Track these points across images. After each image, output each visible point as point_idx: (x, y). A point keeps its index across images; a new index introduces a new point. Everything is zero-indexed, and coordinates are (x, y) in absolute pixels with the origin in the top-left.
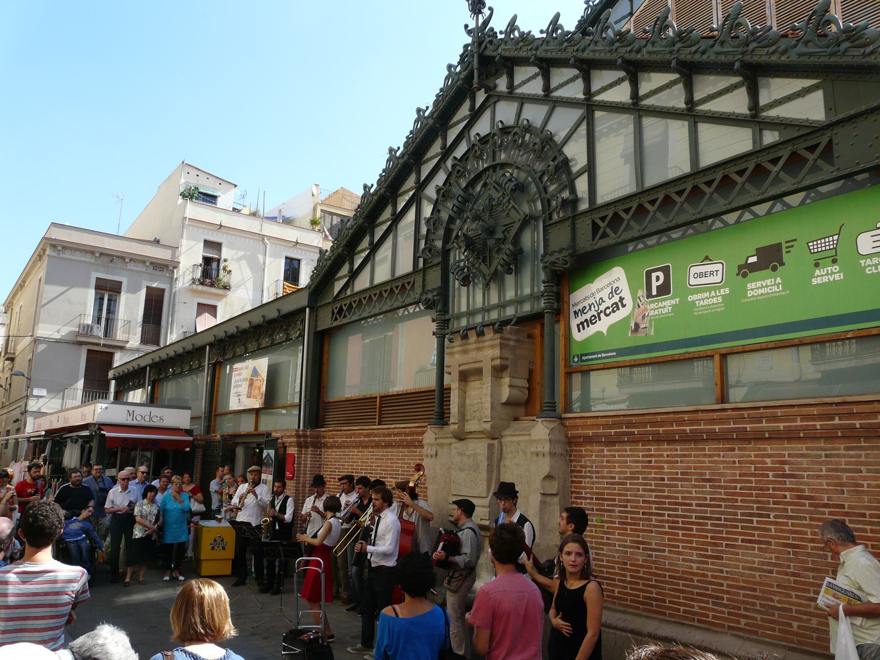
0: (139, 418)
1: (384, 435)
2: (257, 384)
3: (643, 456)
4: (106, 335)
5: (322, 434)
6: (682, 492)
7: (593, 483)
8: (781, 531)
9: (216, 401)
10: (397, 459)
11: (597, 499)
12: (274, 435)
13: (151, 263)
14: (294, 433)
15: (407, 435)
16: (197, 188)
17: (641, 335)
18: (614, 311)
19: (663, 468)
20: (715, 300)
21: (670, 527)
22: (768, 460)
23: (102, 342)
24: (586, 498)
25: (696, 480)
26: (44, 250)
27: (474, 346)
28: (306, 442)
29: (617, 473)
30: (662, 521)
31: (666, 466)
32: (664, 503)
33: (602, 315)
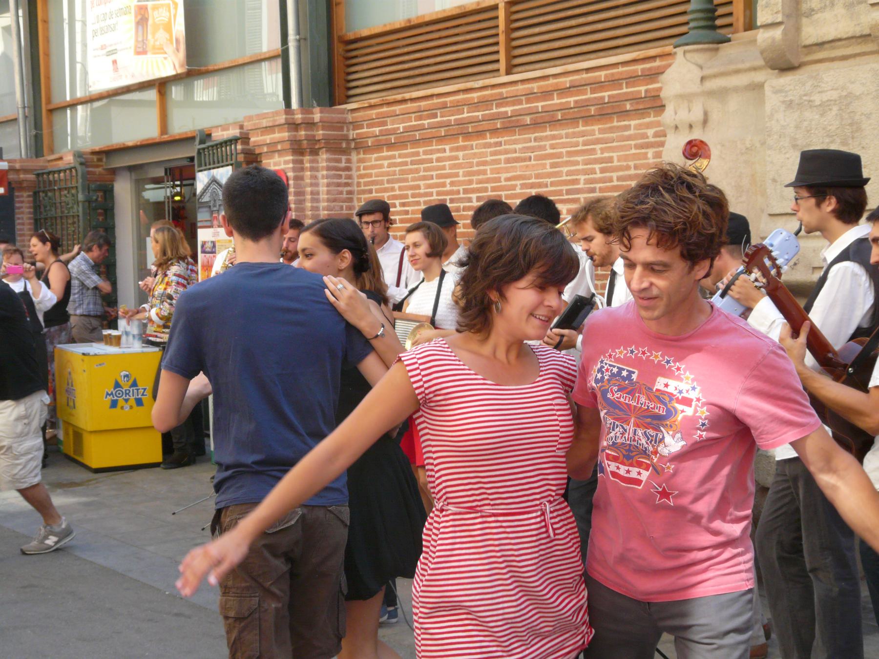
1: (531, 96)
5: (350, 117)
9: (48, 78)
10: (569, 154)
12: (219, 135)
14: (282, 119)
15: (598, 85)
28: (312, 140)
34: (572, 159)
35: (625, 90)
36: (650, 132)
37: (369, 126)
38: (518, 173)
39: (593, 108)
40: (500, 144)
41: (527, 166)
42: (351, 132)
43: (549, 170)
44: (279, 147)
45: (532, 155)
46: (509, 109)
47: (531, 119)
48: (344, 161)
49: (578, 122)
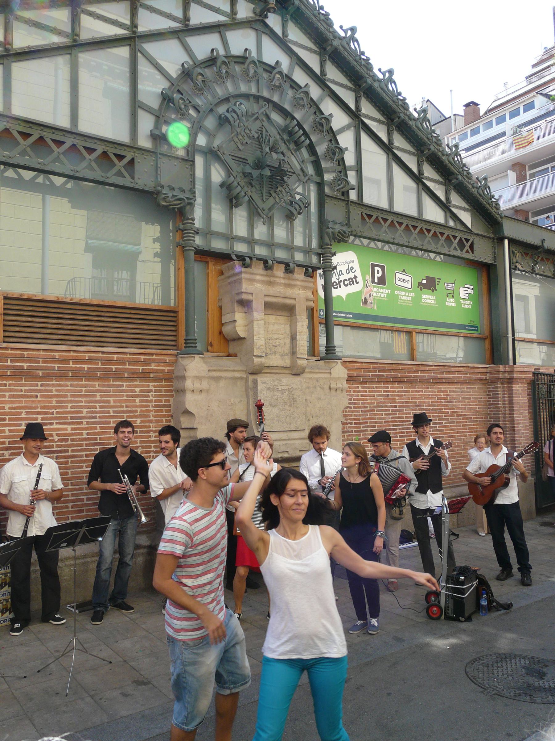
3: (384, 392)
6: (406, 414)
7: (352, 412)
8: (447, 430)
10: (72, 396)
11: (355, 423)
17: (368, 307)
18: (351, 285)
19: (395, 399)
20: (408, 298)
21: (400, 436)
22: (442, 394)
24: (347, 424)
25: (413, 406)
27: (283, 281)
29: (368, 403)
30: (396, 433)
31: (397, 398)
32: (396, 421)
33: (342, 284)
34: (76, 399)
35: (127, 367)
36: (137, 390)
38: (23, 405)
39: (99, 373)
40: (5, 385)
41: (33, 401)
43: (54, 404)
45: (39, 395)
46: (25, 365)
47: (43, 373)
49: (82, 379)
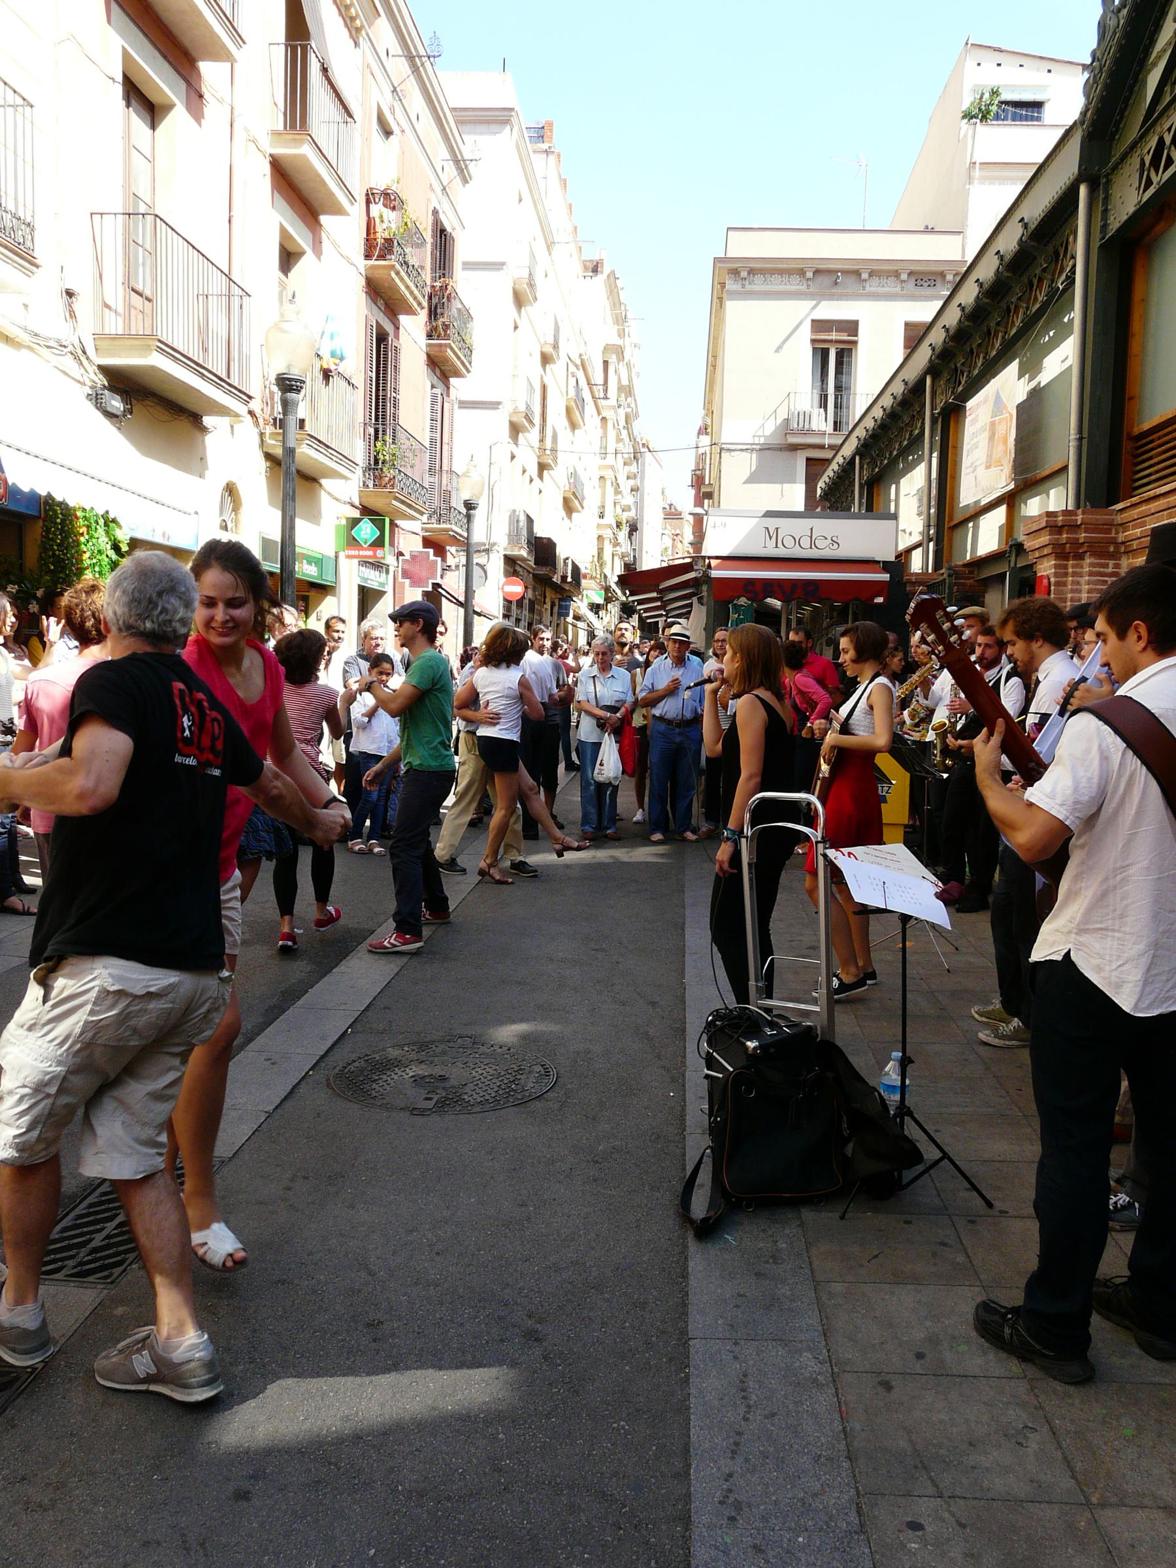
0: (789, 542)
2: (1001, 430)
4: (835, 429)
5: (1119, 519)
9: (952, 498)
13: (910, 274)
16: (995, 93)
23: (827, 441)
26: (723, 285)
28: (1075, 543)
37: (1135, 527)
42: (1120, 535)
44: (1046, 551)
48: (1111, 566)
